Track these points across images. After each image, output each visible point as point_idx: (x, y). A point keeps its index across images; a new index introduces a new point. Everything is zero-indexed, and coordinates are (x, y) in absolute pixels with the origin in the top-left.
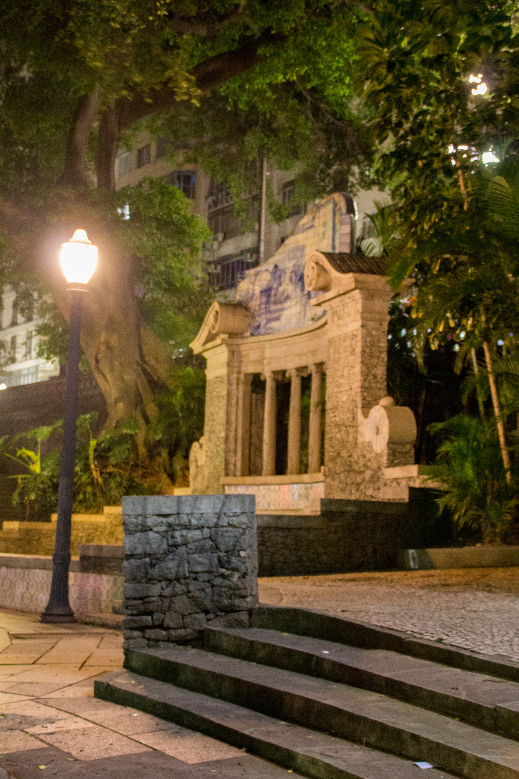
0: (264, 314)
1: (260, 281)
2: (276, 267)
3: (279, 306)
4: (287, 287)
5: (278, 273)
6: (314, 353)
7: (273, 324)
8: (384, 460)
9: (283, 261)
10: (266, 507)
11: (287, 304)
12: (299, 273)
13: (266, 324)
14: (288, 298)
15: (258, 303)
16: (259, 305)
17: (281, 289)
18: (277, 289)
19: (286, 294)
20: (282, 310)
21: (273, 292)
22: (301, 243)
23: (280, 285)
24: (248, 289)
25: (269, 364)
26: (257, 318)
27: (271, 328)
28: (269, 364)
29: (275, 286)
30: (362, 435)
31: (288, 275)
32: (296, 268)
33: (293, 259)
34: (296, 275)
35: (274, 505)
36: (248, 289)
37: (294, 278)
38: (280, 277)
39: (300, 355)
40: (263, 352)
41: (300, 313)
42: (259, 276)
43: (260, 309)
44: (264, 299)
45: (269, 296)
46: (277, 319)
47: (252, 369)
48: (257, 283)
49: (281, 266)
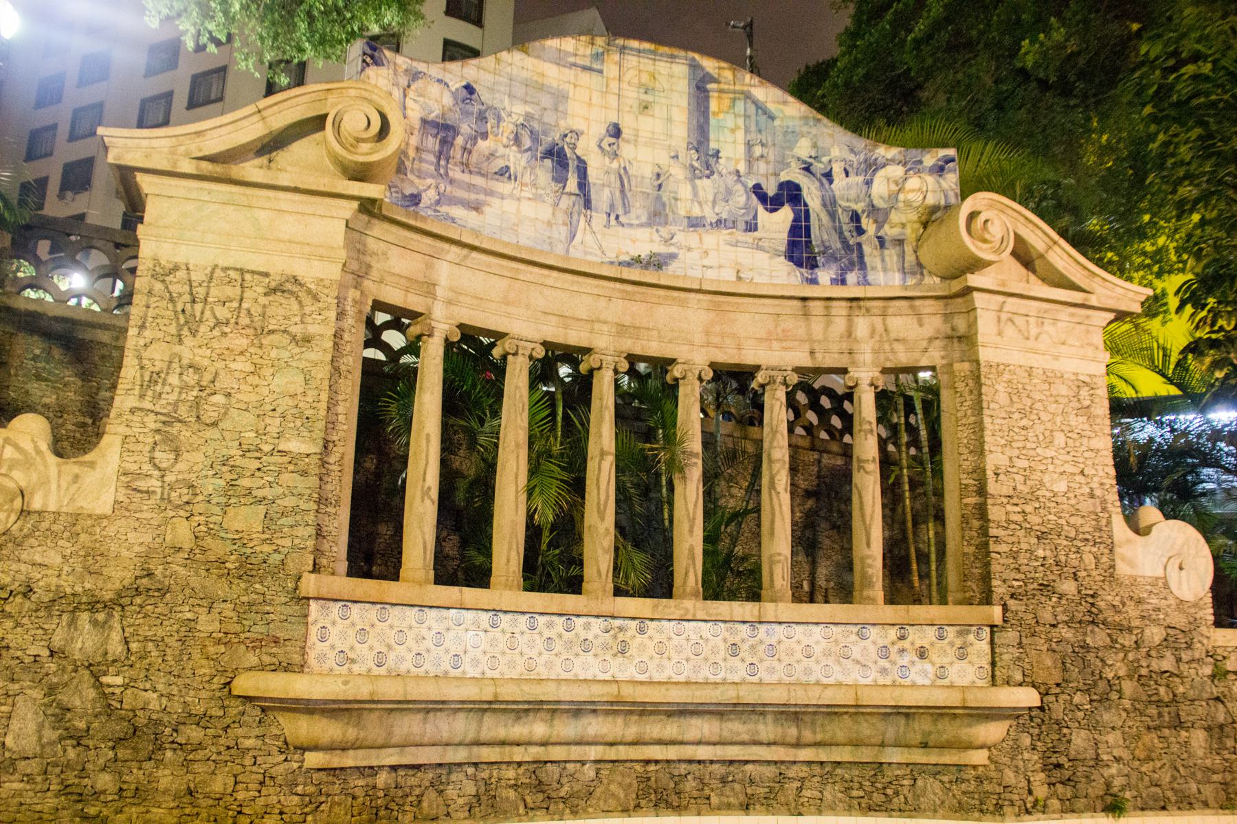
1: (420, 96)
3: (478, 181)
5: (476, 108)
6: (622, 329)
7: (458, 212)
8: (1208, 614)
9: (491, 90)
10: (446, 665)
11: (504, 187)
12: (547, 140)
13: (438, 202)
14: (504, 173)
17: (482, 145)
19: (500, 163)
20: (490, 193)
21: (459, 141)
23: (485, 136)
25: (449, 302)
27: (453, 220)
28: (449, 302)
29: (465, 128)
30: (1131, 564)
31: (507, 128)
32: (536, 126)
35: (475, 662)
37: (527, 142)
38: (482, 118)
39: (565, 319)
40: (429, 266)
41: (549, 224)
43: (421, 160)
45: (446, 143)
46: (477, 208)
47: (394, 296)
49: (485, 96)
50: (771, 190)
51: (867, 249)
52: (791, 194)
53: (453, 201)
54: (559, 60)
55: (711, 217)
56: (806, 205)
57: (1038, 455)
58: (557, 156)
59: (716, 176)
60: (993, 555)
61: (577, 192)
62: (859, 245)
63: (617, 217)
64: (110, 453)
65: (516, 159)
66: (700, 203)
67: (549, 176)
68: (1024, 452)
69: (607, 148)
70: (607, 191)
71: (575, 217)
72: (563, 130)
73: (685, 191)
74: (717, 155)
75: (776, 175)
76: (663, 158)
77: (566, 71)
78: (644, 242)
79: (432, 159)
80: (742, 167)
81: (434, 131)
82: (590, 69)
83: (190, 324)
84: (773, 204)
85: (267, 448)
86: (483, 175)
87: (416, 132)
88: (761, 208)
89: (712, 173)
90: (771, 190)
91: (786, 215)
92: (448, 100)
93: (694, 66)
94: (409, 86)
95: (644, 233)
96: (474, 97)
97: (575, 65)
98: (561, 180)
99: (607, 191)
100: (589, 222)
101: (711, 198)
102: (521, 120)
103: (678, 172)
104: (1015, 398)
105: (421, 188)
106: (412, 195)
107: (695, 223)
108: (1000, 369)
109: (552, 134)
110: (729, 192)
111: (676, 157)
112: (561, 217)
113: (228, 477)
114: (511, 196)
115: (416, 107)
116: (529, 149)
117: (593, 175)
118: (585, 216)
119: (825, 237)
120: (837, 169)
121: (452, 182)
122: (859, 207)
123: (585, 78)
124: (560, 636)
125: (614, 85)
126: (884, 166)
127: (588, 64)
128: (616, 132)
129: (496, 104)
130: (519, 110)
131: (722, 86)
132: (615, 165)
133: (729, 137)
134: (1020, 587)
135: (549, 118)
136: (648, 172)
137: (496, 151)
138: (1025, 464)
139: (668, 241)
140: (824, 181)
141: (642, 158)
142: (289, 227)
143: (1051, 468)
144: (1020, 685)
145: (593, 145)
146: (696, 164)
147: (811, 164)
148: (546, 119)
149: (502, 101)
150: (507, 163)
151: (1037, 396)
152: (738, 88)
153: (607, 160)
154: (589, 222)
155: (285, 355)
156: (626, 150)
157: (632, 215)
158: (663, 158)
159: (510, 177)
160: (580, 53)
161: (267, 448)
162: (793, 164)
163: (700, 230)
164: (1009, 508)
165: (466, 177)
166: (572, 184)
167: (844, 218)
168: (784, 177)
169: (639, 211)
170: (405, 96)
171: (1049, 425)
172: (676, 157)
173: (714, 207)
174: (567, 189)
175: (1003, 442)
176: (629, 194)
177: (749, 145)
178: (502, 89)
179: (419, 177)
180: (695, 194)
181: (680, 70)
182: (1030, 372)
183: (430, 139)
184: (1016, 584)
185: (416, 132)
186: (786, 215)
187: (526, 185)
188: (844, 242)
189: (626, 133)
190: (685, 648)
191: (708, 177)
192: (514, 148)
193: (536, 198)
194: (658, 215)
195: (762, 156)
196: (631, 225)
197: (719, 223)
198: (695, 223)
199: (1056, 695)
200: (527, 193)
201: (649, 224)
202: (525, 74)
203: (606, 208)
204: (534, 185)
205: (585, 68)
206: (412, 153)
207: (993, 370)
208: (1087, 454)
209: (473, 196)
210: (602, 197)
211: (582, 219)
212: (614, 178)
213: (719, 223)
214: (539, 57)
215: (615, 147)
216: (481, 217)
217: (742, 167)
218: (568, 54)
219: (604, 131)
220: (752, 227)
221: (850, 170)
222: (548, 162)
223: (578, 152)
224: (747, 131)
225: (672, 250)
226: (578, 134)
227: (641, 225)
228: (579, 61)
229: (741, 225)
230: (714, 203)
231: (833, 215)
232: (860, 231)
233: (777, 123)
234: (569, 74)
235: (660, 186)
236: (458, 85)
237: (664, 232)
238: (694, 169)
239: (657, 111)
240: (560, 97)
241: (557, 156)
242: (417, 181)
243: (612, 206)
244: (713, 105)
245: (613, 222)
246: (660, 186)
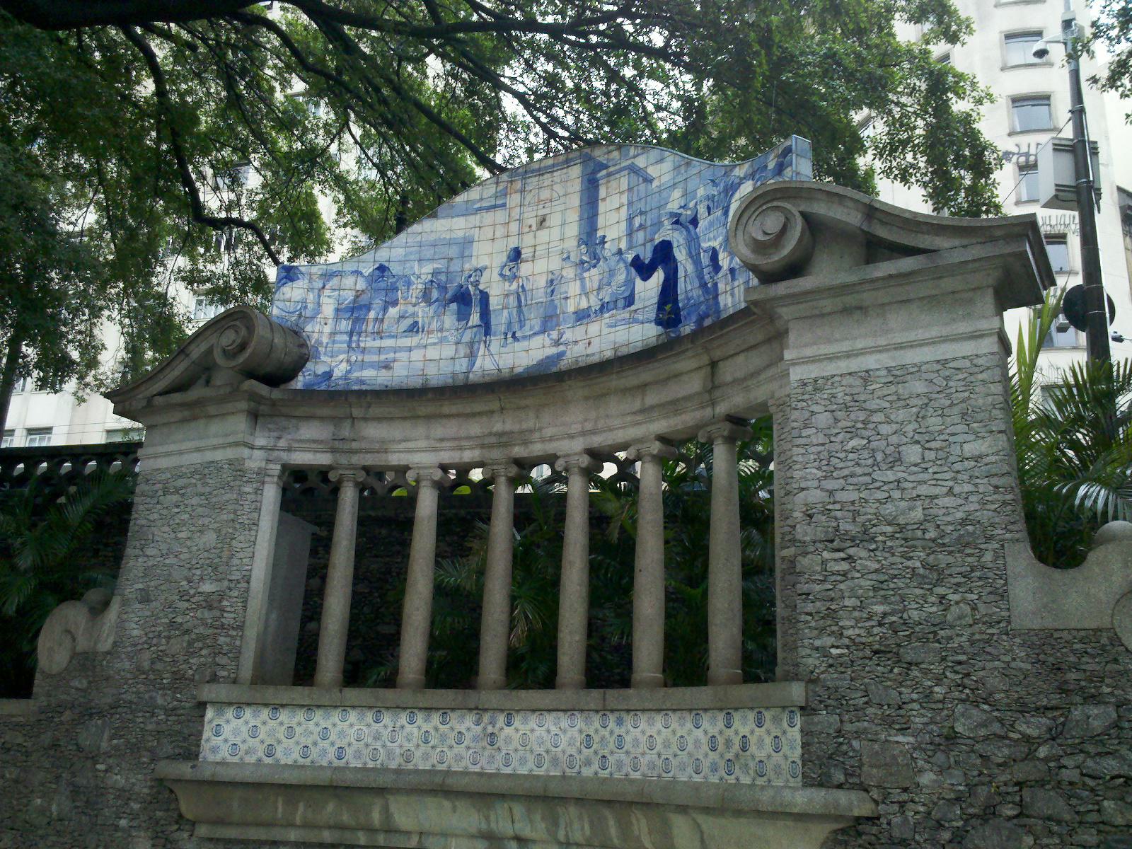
0: (344, 353)
2: (382, 269)
4: (411, 309)
9: (403, 262)
14: (414, 329)
15: (327, 329)
16: (333, 334)
17: (393, 311)
18: (385, 309)
21: (372, 315)
22: (460, 234)
24: (304, 301)
26: (323, 358)
31: (418, 287)
32: (443, 278)
33: (432, 260)
34: (443, 288)
36: (304, 301)
37: (435, 294)
42: (334, 282)
43: (334, 342)
44: (345, 325)
48: (327, 292)
49: (395, 269)
50: (647, 256)
51: (721, 286)
53: (363, 365)
54: (469, 211)
55: (595, 303)
56: (675, 260)
57: (874, 481)
58: (462, 299)
59: (601, 263)
60: (803, 618)
61: (479, 323)
62: (715, 285)
63: (514, 333)
65: (423, 312)
66: (587, 294)
67: (455, 317)
68: (851, 480)
69: (508, 273)
70: (505, 313)
71: (476, 346)
72: (466, 274)
73: (574, 288)
74: (603, 242)
75: (652, 240)
76: (555, 264)
77: (472, 218)
79: (345, 337)
80: (623, 246)
81: (348, 315)
82: (495, 207)
84: (643, 269)
85: (192, 592)
86: (393, 337)
87: (330, 322)
88: (639, 282)
89: (599, 260)
90: (647, 256)
91: (658, 277)
92: (361, 285)
93: (587, 160)
94: (324, 287)
95: (537, 341)
96: (386, 274)
97: (480, 209)
98: (463, 316)
99: (505, 313)
100: (487, 347)
101: (596, 286)
102: (430, 277)
103: (569, 273)
104: (839, 414)
105: (333, 364)
106: (326, 373)
107: (582, 316)
108: (817, 385)
109: (458, 279)
110: (612, 273)
111: (568, 258)
112: (463, 350)
113: (171, 616)
114: (418, 347)
115: (331, 301)
116: (437, 300)
117: (494, 303)
118: (485, 342)
119: (689, 288)
120: (702, 210)
121: (364, 351)
122: (716, 244)
123: (488, 217)
124: (436, 729)
125: (516, 213)
126: (740, 184)
127: (493, 203)
128: (516, 255)
129: (408, 272)
130: (428, 268)
131: (611, 169)
132: (514, 286)
133: (613, 217)
134: (841, 655)
135: (455, 266)
136: (542, 282)
137: (406, 312)
138: (854, 496)
139: (557, 343)
140: (691, 227)
141: (535, 272)
143: (896, 494)
144: (840, 786)
145: (496, 276)
146: (585, 258)
147: (680, 215)
148: (451, 269)
149: (412, 268)
150: (416, 319)
151: (873, 405)
152: (624, 164)
153: (507, 284)
154: (487, 347)
155: (206, 521)
156: (525, 269)
157: (527, 327)
158: (555, 264)
159: (418, 332)
160: (485, 196)
161: (192, 592)
162: (666, 223)
163: (585, 321)
164: (826, 555)
165: (377, 343)
166: (475, 318)
167: (705, 259)
168: (658, 239)
169: (534, 322)
170: (319, 296)
171: (894, 439)
172: (568, 258)
173: (598, 294)
174: (470, 324)
175: (820, 474)
176: (525, 309)
177: (630, 219)
178: (412, 257)
179: (332, 357)
180: (583, 286)
182: (866, 377)
183: (344, 322)
184: (834, 651)
185: (330, 322)
186: (658, 277)
187: (433, 332)
188: (703, 285)
189: (526, 253)
190: (543, 739)
191: (595, 266)
192: (423, 304)
193: (442, 341)
194: (549, 321)
195: (641, 225)
196: (525, 337)
197: (603, 308)
198: (582, 316)
199: (902, 804)
200: (433, 338)
201: (543, 332)
202: (433, 237)
203: (503, 329)
204: (441, 330)
205: (488, 209)
206: (325, 340)
207: (810, 388)
208: (958, 466)
209: (383, 357)
210: (499, 321)
211: (482, 346)
212: (512, 301)
213: (603, 308)
214: (444, 218)
215: (515, 270)
216: (389, 373)
217: (623, 246)
218: (475, 202)
219: (505, 259)
220: (630, 301)
221: (711, 206)
222: (454, 306)
223: (481, 287)
224: (630, 204)
225: (562, 348)
226: (480, 271)
227: (535, 334)
228: (485, 204)
229: (621, 303)
230: (599, 289)
231: (697, 262)
232: (716, 267)
233: (655, 184)
234: (474, 220)
235: (553, 291)
236: (371, 270)
237: (554, 335)
238: (583, 262)
239: (554, 220)
241: (462, 299)
242: (329, 360)
243: (509, 324)
244: (602, 192)
245: (510, 340)
246: (553, 291)
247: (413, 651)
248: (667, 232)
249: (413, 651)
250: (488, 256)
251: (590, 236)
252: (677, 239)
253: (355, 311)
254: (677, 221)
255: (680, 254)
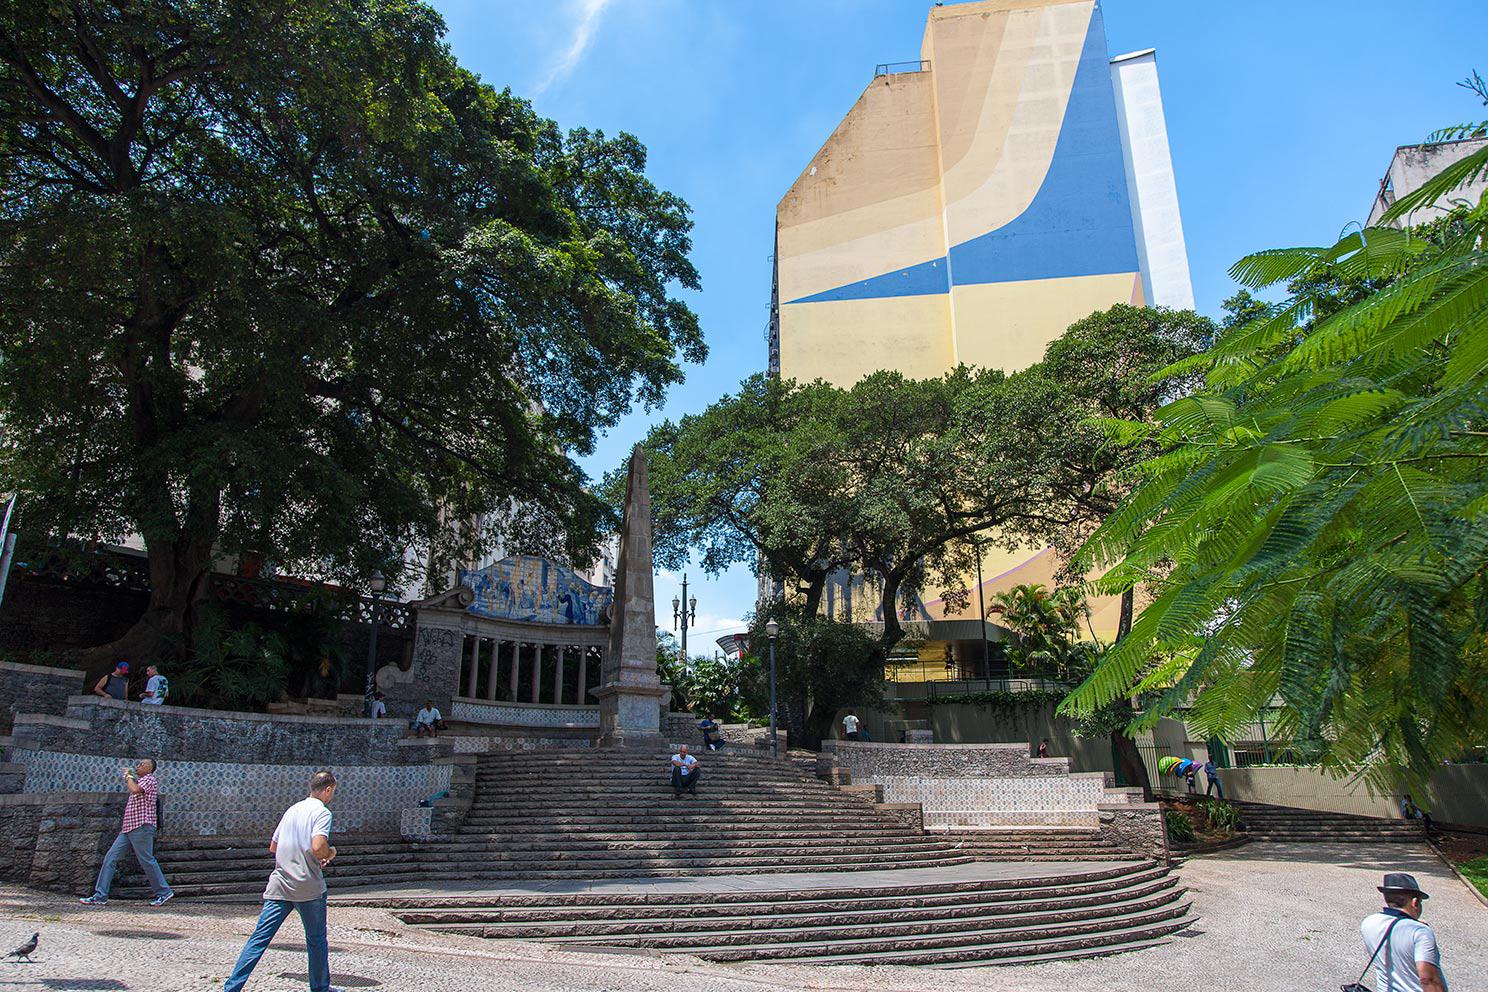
14: (494, 597)
50: (562, 596)
52: (567, 598)
64: (411, 671)
65: (496, 592)
78: (528, 613)
83: (428, 642)
84: (563, 601)
91: (566, 603)
107: (542, 607)
128: (522, 582)
142: (449, 619)
181: (541, 563)
194: (532, 605)
198: (542, 607)
210: (518, 601)
213: (549, 606)
240: (508, 574)
247: (493, 692)
248: (569, 593)
249: (493, 692)
250: (514, 581)
251: (545, 583)
252: (573, 596)
253: (479, 588)
254: (573, 591)
255: (574, 601)
